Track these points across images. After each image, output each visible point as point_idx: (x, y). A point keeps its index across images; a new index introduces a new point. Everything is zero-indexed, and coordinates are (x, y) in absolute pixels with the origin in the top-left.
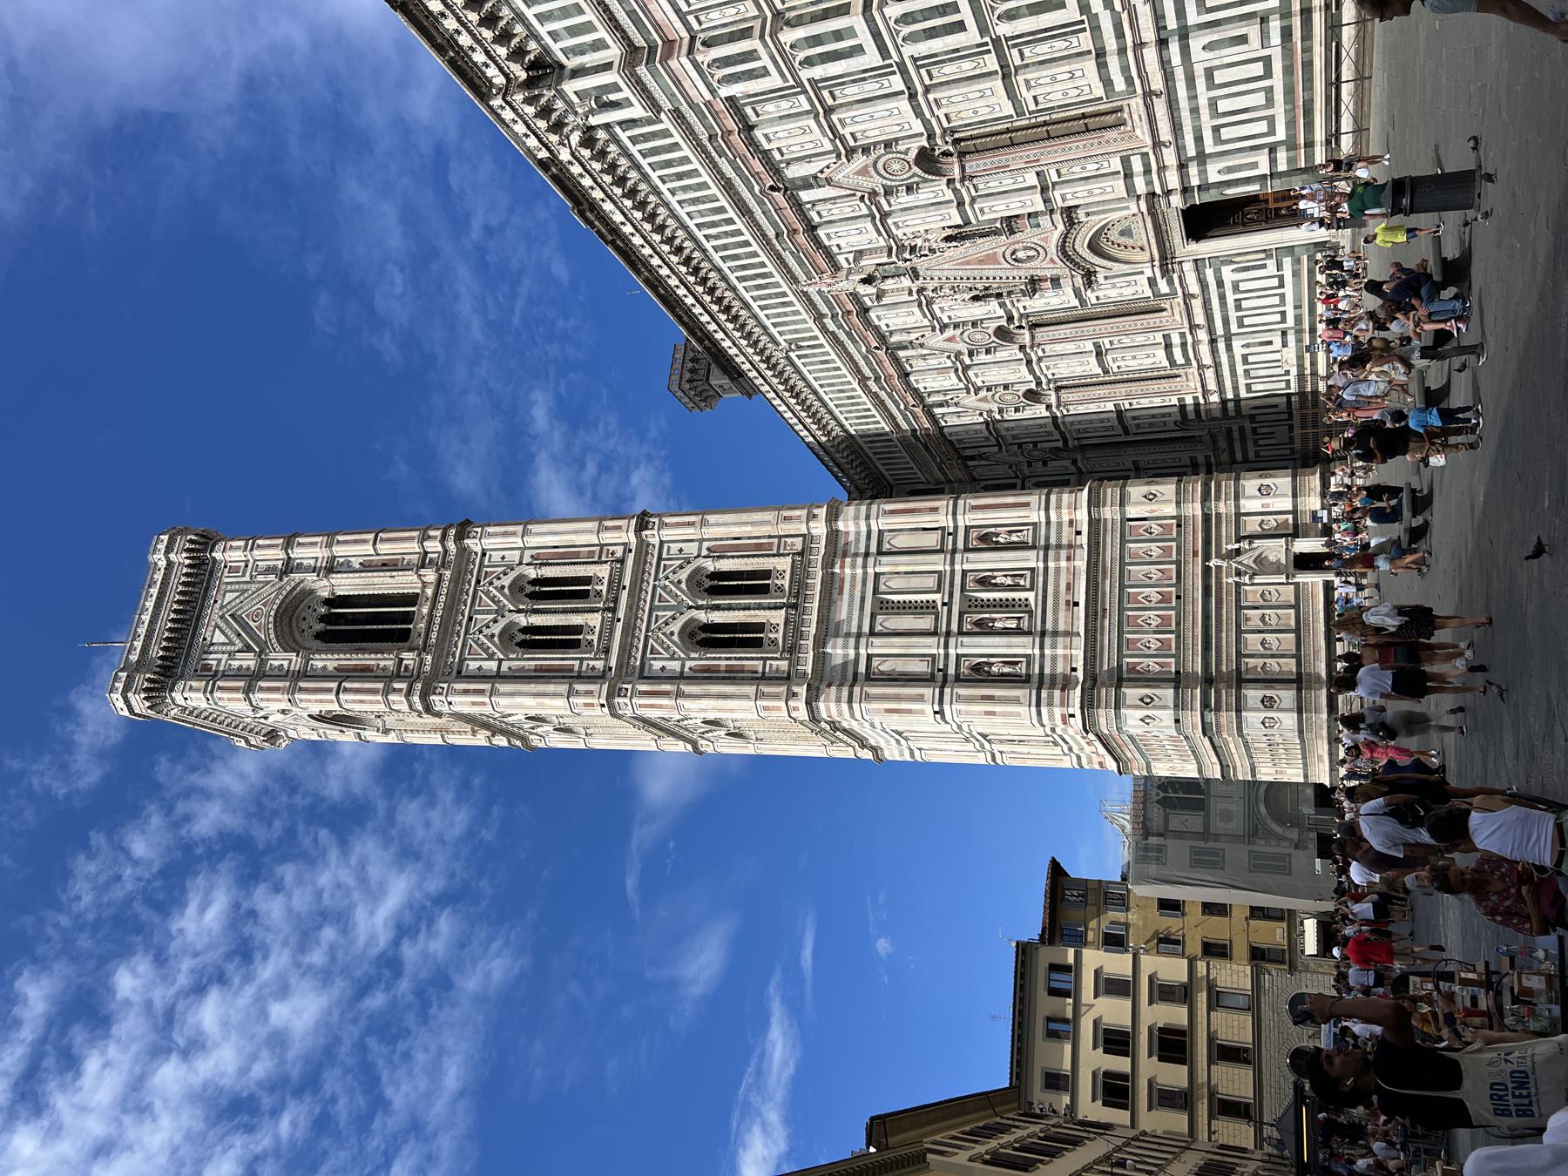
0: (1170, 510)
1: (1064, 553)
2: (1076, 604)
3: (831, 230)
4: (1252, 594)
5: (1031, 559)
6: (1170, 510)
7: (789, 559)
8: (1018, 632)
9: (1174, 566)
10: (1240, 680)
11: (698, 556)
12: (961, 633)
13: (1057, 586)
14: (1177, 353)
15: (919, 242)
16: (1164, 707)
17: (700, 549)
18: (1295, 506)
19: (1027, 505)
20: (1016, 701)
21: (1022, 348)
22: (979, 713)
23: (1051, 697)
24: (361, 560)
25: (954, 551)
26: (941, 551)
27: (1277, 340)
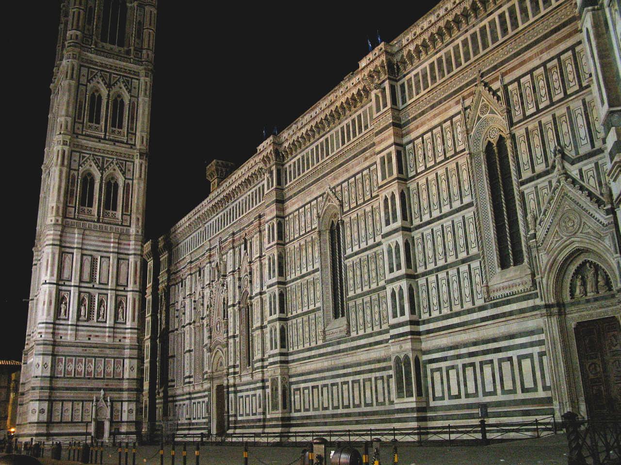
0: (126, 376)
1: (111, 334)
2: (89, 339)
3: (232, 255)
4: (89, 406)
5: (110, 322)
6: (126, 376)
7: (120, 218)
8: (79, 315)
9: (102, 377)
10: (51, 401)
11: (125, 178)
12: (80, 292)
13: (97, 332)
14: (187, 380)
15: (225, 288)
16: (42, 372)
17: (129, 179)
18: (124, 422)
19: (134, 320)
20: (49, 314)
21: (194, 322)
22: (44, 299)
23: (50, 328)
24: (141, 21)
25: (116, 290)
26: (117, 285)
27: (188, 417)
